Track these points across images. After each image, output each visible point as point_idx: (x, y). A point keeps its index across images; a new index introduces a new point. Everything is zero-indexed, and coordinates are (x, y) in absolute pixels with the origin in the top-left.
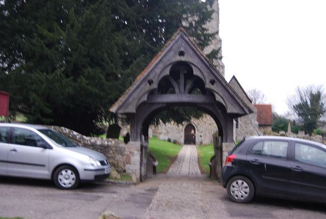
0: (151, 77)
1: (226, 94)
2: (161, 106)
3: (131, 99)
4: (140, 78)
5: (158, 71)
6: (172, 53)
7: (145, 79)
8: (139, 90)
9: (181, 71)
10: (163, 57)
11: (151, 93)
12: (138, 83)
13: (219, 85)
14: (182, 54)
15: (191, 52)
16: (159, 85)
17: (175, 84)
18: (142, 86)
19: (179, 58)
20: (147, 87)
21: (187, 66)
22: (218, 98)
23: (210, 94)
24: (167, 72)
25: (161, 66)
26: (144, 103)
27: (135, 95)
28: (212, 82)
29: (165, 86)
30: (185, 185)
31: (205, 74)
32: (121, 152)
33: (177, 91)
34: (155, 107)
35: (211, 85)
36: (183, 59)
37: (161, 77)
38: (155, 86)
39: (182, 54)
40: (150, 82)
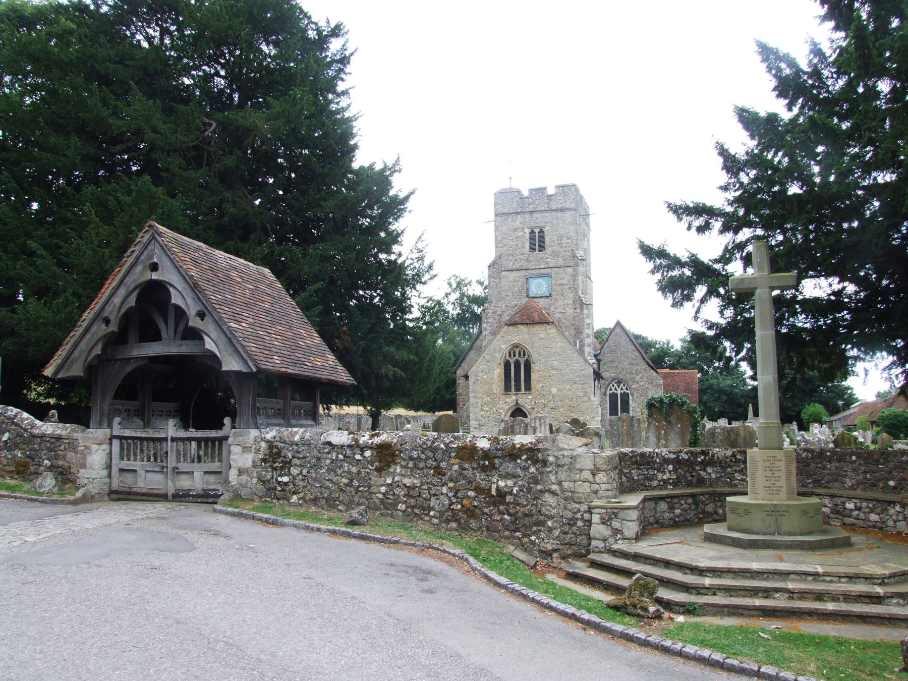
0: (106, 313)
1: (222, 336)
3: (76, 354)
4: (88, 316)
5: (117, 300)
6: (139, 268)
8: (88, 337)
10: (125, 276)
12: (85, 324)
13: (211, 317)
14: (154, 267)
15: (169, 264)
18: (94, 329)
20: (101, 330)
22: (209, 345)
24: (132, 302)
25: (122, 292)
27: (83, 345)
28: (201, 315)
30: (539, 292)
31: (189, 301)
32: (72, 445)
33: (164, 335)
35: (198, 319)
36: (155, 276)
37: (123, 311)
39: (154, 267)
40: (107, 321)
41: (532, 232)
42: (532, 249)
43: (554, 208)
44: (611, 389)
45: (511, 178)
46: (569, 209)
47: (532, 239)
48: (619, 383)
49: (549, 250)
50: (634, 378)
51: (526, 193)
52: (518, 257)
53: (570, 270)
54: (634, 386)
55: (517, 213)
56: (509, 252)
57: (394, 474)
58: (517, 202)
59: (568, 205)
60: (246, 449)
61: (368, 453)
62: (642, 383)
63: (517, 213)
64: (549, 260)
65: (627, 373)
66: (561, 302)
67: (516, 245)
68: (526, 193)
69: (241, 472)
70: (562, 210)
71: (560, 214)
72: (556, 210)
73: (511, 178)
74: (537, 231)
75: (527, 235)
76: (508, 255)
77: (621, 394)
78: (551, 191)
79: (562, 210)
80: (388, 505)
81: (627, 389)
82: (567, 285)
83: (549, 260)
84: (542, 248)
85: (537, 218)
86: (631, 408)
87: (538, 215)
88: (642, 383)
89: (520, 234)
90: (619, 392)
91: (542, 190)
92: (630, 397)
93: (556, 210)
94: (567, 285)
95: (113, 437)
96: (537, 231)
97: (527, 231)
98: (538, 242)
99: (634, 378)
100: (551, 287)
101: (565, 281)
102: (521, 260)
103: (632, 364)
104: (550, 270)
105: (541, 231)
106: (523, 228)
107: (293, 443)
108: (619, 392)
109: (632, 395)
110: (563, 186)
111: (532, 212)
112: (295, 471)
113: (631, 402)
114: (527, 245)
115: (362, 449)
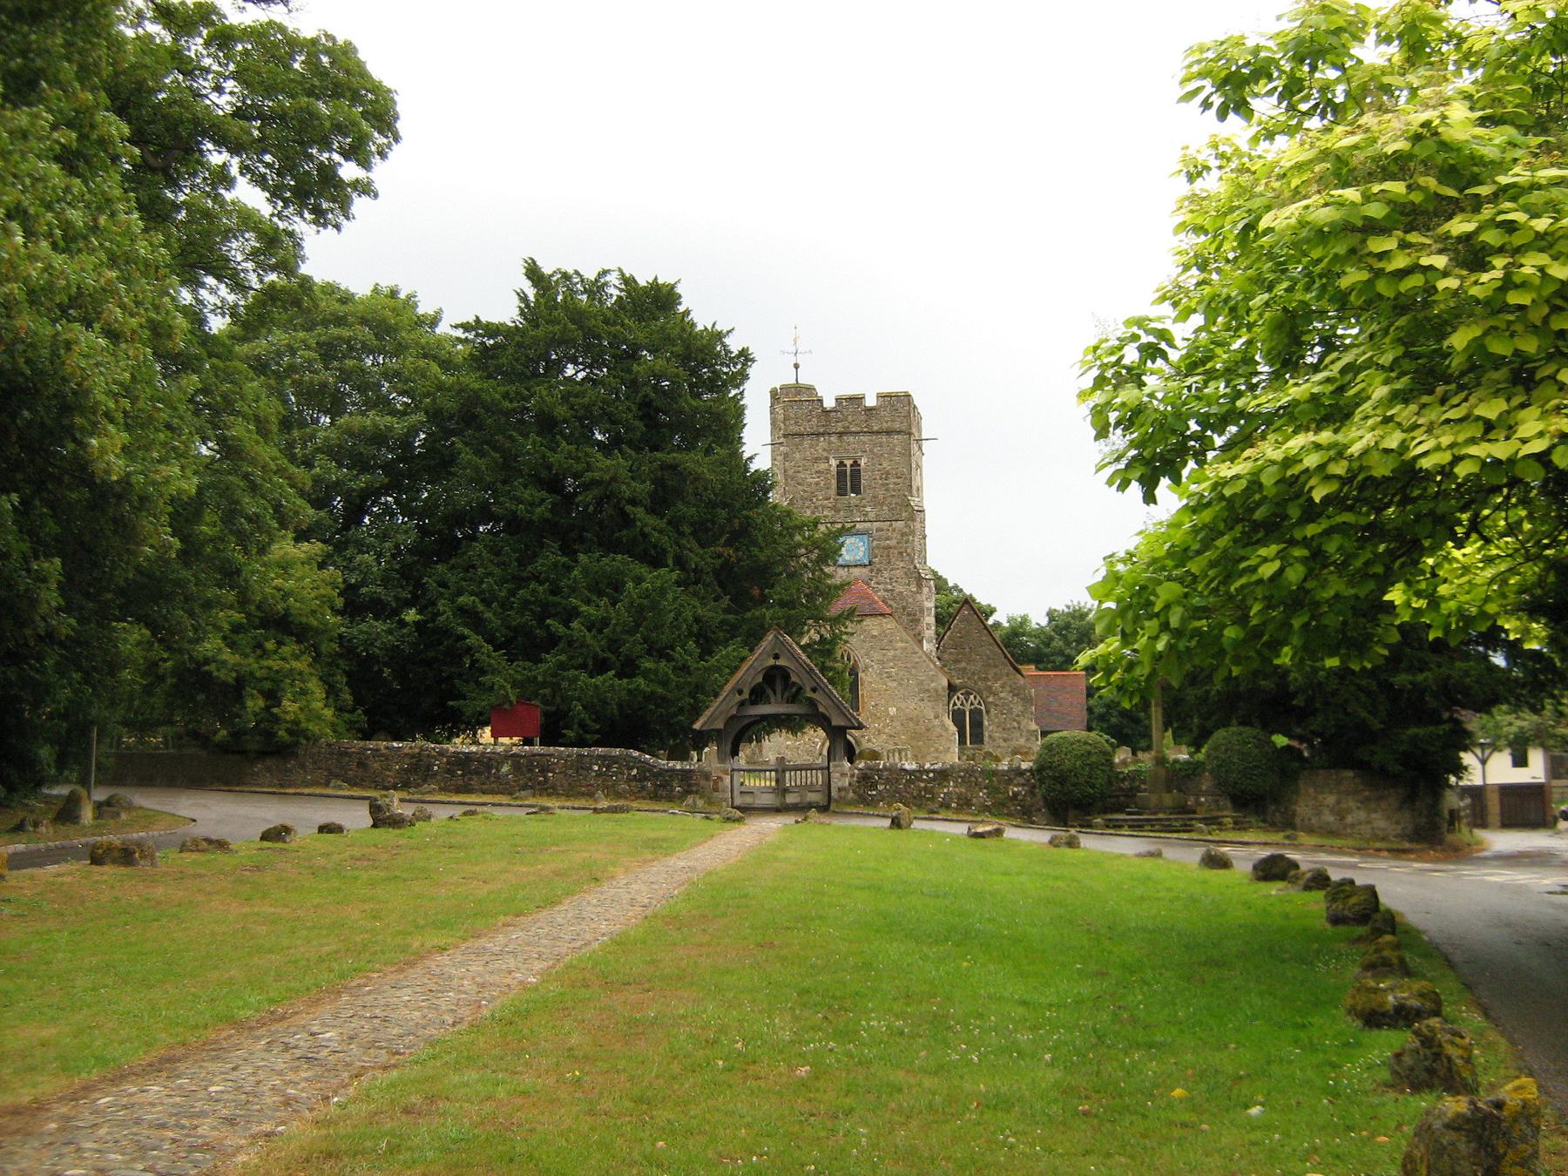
2: (752, 719)
4: (728, 687)
7: (733, 688)
9: (775, 678)
11: (742, 704)
14: (776, 657)
16: (751, 695)
17: (769, 691)
19: (771, 662)
21: (784, 673)
22: (821, 709)
23: (812, 703)
24: (760, 679)
25: (752, 672)
26: (733, 717)
28: (814, 690)
29: (758, 695)
30: (852, 558)
34: (746, 721)
38: (746, 696)
40: (740, 692)
41: (841, 464)
42: (841, 491)
43: (875, 428)
44: (955, 704)
45: (796, 366)
46: (899, 432)
47: (841, 474)
48: (967, 694)
49: (867, 494)
50: (990, 687)
51: (829, 403)
52: (820, 503)
53: (900, 524)
54: (991, 699)
55: (818, 435)
56: (806, 495)
57: (948, 787)
58: (818, 417)
59: (897, 426)
60: (843, 775)
61: (931, 775)
62: (1002, 695)
63: (818, 435)
64: (868, 509)
65: (980, 678)
66: (886, 574)
67: (817, 484)
68: (829, 403)
69: (840, 790)
70: (889, 433)
71: (884, 439)
72: (878, 433)
73: (796, 366)
74: (848, 463)
75: (834, 469)
76: (803, 499)
77: (971, 711)
78: (871, 401)
79: (889, 433)
80: (946, 805)
81: (979, 703)
82: (895, 548)
83: (868, 509)
84: (856, 489)
85: (849, 444)
86: (986, 734)
87: (851, 439)
88: (1002, 695)
89: (823, 466)
90: (967, 708)
91: (857, 400)
92: (985, 717)
93: (878, 433)
94: (895, 548)
95: (733, 770)
96: (848, 463)
97: (834, 463)
98: (848, 480)
99: (990, 687)
100: (872, 552)
101: (892, 543)
102: (824, 507)
103: (989, 665)
104: (869, 524)
105: (855, 464)
106: (827, 459)
107: (879, 770)
108: (967, 708)
109: (988, 712)
110: (889, 396)
111: (841, 434)
112: (881, 787)
113: (986, 723)
114: (834, 482)
115: (928, 772)
